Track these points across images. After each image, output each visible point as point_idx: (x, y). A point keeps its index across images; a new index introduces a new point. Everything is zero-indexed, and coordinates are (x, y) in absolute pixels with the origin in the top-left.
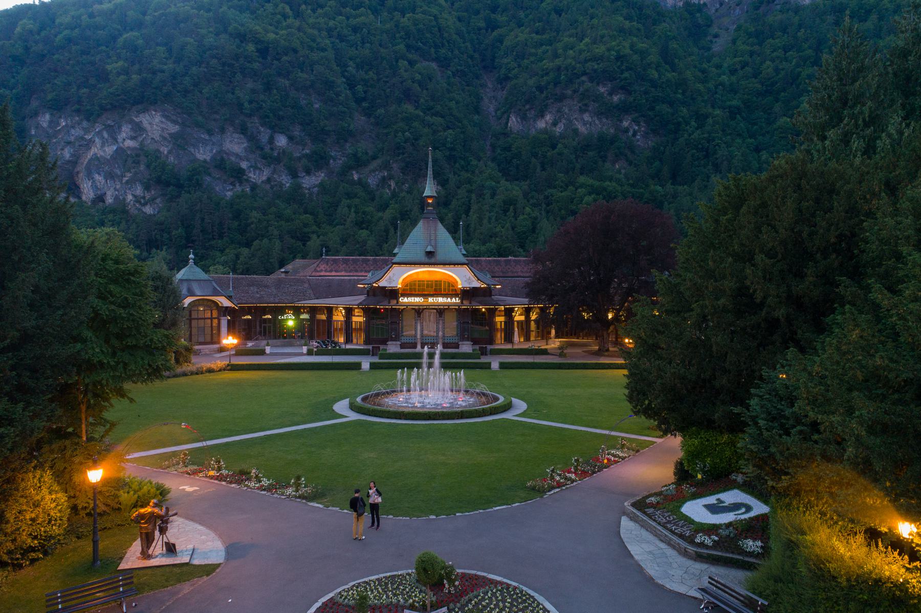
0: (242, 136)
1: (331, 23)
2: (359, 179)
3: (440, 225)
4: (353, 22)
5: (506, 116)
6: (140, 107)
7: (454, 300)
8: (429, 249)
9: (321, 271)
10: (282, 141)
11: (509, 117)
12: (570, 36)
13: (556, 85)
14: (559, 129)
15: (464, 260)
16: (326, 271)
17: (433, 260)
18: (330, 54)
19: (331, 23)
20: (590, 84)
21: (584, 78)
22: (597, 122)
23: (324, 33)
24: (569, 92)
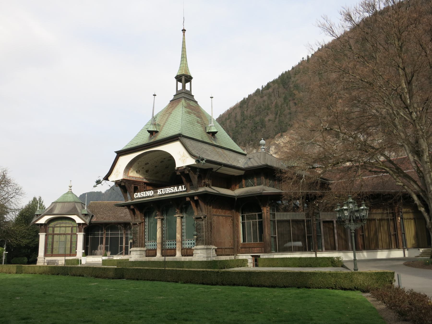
6: (279, 135)
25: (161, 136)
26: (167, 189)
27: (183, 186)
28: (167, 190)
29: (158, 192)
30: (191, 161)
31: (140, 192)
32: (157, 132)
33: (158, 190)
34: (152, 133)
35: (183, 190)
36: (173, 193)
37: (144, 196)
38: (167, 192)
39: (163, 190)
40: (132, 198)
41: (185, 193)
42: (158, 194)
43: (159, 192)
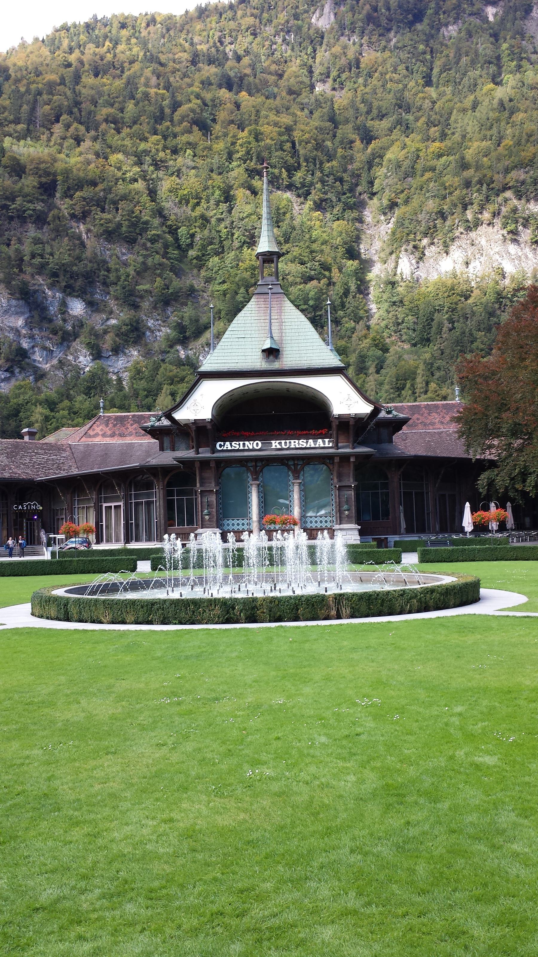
0: (21, 302)
1: (143, 146)
2: (187, 357)
3: (288, 306)
4: (171, 142)
5: (394, 256)
7: (320, 443)
8: (267, 345)
9: (97, 435)
10: (77, 308)
11: (398, 257)
12: (484, 138)
13: (465, 208)
14: (477, 269)
15: (334, 361)
16: (104, 435)
17: (276, 366)
18: (140, 185)
19: (143, 146)
20: (515, 202)
21: (508, 194)
22: (531, 255)
23: (132, 159)
24: (486, 216)
25: (290, 359)
26: (292, 441)
27: (327, 440)
28: (293, 444)
29: (274, 445)
30: (366, 409)
31: (231, 441)
32: (277, 351)
33: (273, 442)
34: (272, 353)
35: (327, 445)
36: (306, 448)
37: (241, 448)
38: (292, 446)
39: (283, 442)
40: (214, 451)
41: (331, 451)
42: (273, 447)
43: (275, 444)
